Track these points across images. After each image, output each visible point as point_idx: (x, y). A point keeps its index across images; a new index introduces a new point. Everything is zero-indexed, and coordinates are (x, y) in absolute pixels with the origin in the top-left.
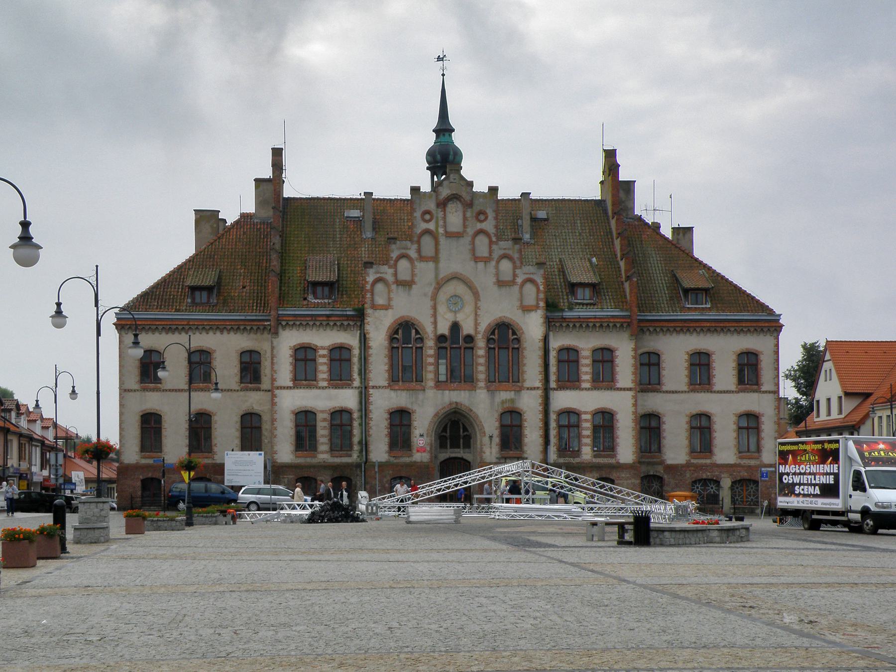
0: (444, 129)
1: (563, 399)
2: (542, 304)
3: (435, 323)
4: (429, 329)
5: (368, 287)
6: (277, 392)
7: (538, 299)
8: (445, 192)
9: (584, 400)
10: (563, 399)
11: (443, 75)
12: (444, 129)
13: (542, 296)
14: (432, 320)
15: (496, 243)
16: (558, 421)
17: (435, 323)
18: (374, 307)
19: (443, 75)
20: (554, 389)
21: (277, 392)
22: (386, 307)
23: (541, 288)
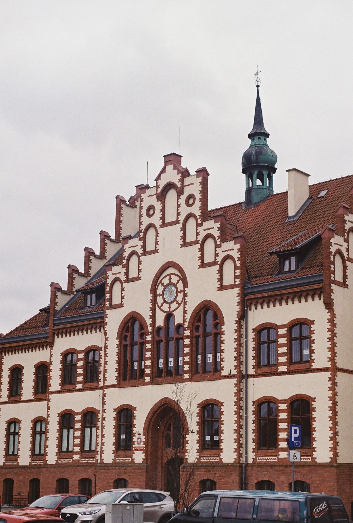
0: (259, 133)
1: (261, 388)
2: (238, 281)
3: (153, 317)
4: (149, 322)
5: (108, 289)
6: (51, 396)
7: (236, 277)
8: (162, 183)
9: (282, 387)
10: (261, 388)
11: (258, 86)
12: (259, 133)
13: (238, 272)
14: (150, 313)
15: (201, 225)
16: (258, 412)
17: (153, 317)
18: (112, 307)
19: (258, 86)
20: (253, 376)
21: (51, 396)
22: (121, 305)
23: (238, 264)
